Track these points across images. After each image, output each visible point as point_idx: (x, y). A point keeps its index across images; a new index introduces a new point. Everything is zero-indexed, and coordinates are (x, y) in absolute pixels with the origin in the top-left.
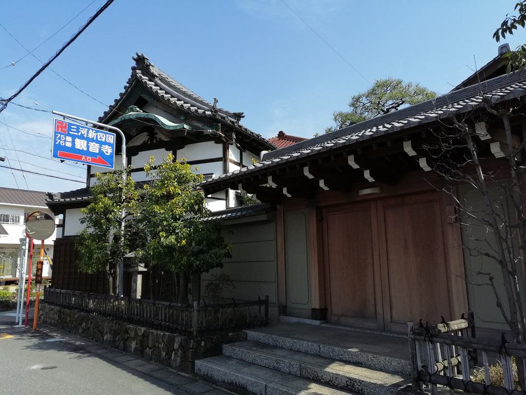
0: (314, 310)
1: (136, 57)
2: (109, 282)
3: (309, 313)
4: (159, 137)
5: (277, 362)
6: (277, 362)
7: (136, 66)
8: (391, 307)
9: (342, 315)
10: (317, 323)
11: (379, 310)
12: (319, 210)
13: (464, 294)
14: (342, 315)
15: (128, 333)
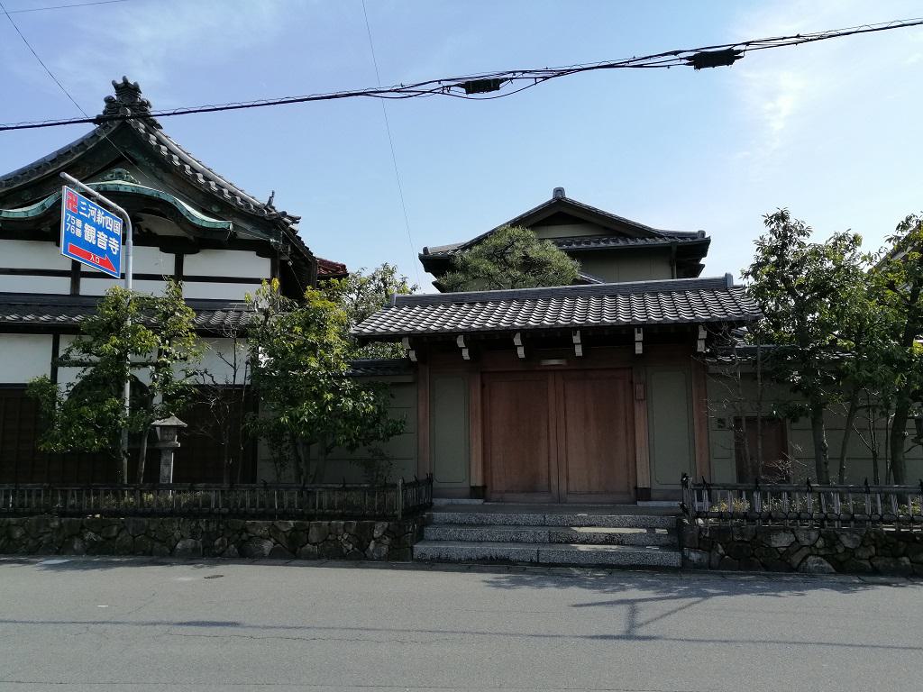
0: (473, 488)
1: (120, 81)
2: (123, 464)
3: (468, 491)
4: (146, 226)
5: (516, 534)
6: (516, 534)
7: (115, 97)
8: (568, 479)
9: (506, 491)
10: (480, 501)
11: (554, 482)
12: (482, 373)
13: (887, 443)
14: (506, 491)
15: (247, 532)
